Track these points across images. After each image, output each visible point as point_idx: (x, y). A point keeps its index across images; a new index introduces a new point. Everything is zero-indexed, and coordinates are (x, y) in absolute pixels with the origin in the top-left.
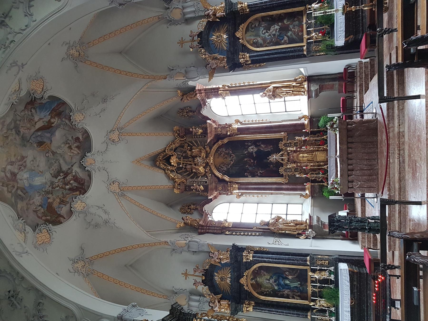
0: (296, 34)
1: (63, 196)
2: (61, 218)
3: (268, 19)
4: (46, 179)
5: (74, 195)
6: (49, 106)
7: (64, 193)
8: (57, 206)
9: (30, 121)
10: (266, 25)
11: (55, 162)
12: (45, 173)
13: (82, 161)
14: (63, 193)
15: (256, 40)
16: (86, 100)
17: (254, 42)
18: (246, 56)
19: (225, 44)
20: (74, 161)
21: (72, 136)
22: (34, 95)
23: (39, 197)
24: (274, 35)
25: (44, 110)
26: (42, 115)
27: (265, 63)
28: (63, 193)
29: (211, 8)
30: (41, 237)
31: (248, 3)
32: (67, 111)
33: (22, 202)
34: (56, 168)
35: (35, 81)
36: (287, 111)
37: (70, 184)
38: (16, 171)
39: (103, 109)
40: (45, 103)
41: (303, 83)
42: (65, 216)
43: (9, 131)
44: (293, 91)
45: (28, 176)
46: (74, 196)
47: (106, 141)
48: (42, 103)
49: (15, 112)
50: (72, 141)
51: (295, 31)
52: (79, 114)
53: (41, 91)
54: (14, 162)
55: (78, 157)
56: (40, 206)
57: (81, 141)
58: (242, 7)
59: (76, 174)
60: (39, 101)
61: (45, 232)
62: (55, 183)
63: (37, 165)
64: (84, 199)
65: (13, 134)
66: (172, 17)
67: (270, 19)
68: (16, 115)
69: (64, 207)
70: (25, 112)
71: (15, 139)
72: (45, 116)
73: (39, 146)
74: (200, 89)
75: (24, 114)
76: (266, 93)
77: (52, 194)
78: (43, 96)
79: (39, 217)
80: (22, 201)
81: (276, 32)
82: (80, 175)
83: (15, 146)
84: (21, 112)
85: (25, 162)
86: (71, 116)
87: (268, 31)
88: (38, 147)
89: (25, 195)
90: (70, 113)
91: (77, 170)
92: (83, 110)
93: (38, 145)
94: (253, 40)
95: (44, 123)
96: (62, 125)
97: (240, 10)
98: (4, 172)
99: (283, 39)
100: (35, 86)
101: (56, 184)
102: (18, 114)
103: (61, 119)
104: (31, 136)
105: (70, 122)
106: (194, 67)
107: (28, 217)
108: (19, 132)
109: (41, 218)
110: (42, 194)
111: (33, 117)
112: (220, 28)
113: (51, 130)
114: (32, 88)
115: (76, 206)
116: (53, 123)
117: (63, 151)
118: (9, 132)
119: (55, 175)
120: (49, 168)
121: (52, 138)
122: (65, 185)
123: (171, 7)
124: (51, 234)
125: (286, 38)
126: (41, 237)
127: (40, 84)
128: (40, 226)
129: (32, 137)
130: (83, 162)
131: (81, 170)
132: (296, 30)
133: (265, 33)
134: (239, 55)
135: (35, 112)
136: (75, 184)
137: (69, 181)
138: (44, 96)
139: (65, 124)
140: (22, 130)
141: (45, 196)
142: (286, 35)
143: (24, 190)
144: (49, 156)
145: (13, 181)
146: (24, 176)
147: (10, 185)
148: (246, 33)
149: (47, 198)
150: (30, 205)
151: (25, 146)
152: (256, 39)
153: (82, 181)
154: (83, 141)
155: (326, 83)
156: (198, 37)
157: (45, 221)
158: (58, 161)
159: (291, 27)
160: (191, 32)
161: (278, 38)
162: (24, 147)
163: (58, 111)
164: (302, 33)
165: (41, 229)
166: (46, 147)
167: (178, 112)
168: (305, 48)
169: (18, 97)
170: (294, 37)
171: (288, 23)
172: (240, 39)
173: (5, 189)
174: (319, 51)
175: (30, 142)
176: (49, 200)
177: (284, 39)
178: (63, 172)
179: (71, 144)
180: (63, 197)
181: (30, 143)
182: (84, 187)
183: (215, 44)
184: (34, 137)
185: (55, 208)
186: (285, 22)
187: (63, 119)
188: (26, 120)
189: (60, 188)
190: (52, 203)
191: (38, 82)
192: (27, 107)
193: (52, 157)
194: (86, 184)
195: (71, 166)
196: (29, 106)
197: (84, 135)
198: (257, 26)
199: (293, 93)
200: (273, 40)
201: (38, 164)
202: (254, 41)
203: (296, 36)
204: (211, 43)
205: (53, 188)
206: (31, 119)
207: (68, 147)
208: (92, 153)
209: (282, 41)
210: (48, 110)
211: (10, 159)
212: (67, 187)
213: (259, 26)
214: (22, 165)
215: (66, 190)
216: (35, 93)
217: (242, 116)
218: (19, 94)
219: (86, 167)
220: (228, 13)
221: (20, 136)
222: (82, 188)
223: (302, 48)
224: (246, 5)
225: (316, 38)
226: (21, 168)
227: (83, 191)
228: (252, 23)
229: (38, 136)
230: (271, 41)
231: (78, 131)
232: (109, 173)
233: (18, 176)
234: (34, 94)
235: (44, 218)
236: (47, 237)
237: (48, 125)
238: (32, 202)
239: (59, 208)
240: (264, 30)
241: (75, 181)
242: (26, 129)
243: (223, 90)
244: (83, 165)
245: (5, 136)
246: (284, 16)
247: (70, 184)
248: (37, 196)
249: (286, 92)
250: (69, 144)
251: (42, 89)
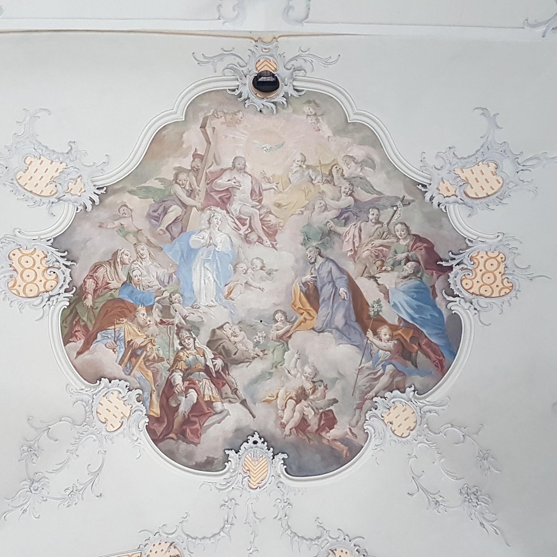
1: (151, 358)
2: (80, 343)
4: (206, 309)
5: (151, 396)
6: (429, 317)
7: (159, 364)
8: (122, 334)
9: (377, 256)
11: (257, 344)
12: (225, 307)
13: (258, 440)
14: (161, 359)
16: (461, 434)
20: (260, 410)
21: (337, 401)
22: (458, 264)
23: (157, 278)
25: (415, 303)
26: (400, 298)
28: (161, 359)
30: (34, 265)
32: (418, 380)
33: (146, 214)
34: (239, 346)
35: (501, 269)
37: (187, 389)
38: (235, 207)
39: (440, 499)
40: (435, 307)
42: (86, 356)
43: (347, 184)
45: (219, 248)
46: (146, 395)
47: (326, 536)
48: (435, 295)
49: (403, 200)
50: (321, 403)
52: (413, 419)
53: (471, 291)
54: (260, 201)
55: (271, 427)
56: (130, 278)
57: (323, 434)
59: (217, 413)
60: (439, 284)
61: (45, 284)
62: (195, 339)
63: (250, 281)
64: (134, 430)
65: (338, 200)
68: (393, 206)
69: (115, 356)
70: (405, 238)
71: (326, 208)
72: (395, 306)
73: (304, 289)
75: (398, 234)
77: (162, 322)
78: (458, 296)
79: (96, 267)
80: (149, 216)
82: (212, 428)
83: (305, 207)
84: (401, 223)
85: (260, 240)
86: (404, 392)
88: (301, 285)
89: (164, 229)
90: (413, 389)
91: (228, 416)
92: (428, 427)
93: (308, 289)
95: (376, 305)
96: (371, 362)
98: (234, 166)
100: (484, 270)
101: (192, 340)
102: (396, 211)
103: (391, 358)
104: (332, 261)
105: (384, 389)
107: (100, 227)
108: (347, 219)
109: (92, 277)
110: (163, 289)
111: (390, 269)
113: (354, 328)
114: (478, 257)
115: (113, 397)
116: (375, 333)
117: (292, 372)
118: (345, 186)
119: (221, 339)
120: (240, 323)
121: (331, 332)
122: (187, 370)
124: (37, 301)
126: (34, 265)
127: (494, 286)
128: (67, 266)
129: (331, 264)
130: (255, 442)
131: (230, 435)
135: (405, 274)
136: (184, 407)
137: (195, 384)
138: (457, 299)
139: (375, 374)
140: (351, 230)
141: (157, 298)
143: (180, 230)
144: (278, 322)
145: (207, 194)
146: (220, 233)
147: (195, 184)
149: (151, 303)
150: (135, 244)
151: (307, 239)
153: (191, 430)
154: (325, 442)
157: (81, 287)
158: (261, 354)
162: (302, 238)
163: (416, 348)
165: (59, 268)
166: (302, 314)
169: (447, 198)
173: (187, 163)
175: (315, 260)
176: (142, 310)
178: (225, 368)
179: (311, 397)
180: (146, 359)
181: (313, 260)
182: (171, 435)
184: (330, 272)
185: (117, 326)
187: (389, 368)
188: (380, 241)
189: (178, 352)
190: (133, 319)
191: (499, 276)
192: (419, 244)
193: (274, 334)
194: (183, 446)
195: (244, 398)
196: (423, 251)
197: (342, 446)
201: (254, 284)
205: (179, 328)
206: (383, 262)
207: (303, 389)
208: (283, 479)
210: (416, 316)
211: (270, 189)
212: (178, 377)
214: (252, 230)
215: (169, 370)
216: (462, 269)
218: (456, 202)
219: (236, 453)
221: (332, 223)
222: (169, 429)
226: (244, 225)
227: (159, 429)
229: (334, 286)
231: (354, 422)
232: (212, 540)
233: (220, 213)
234: (461, 266)
235: (90, 285)
236: (29, 287)
237: (369, 317)
238: (142, 252)
239: (116, 340)
241: (196, 403)
242: (354, 243)
244: (245, 444)
245: (334, 171)
247: (187, 389)
248: (161, 272)
250: (313, 392)
251: (478, 293)
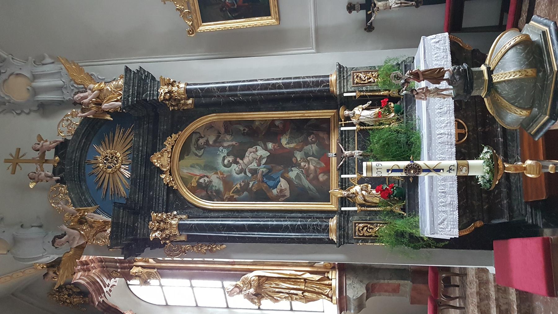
0: (312, 176)
3: (242, 128)
10: (234, 143)
15: (207, 179)
17: (199, 185)
18: (171, 224)
19: (124, 180)
24: (254, 172)
27: (224, 246)
29: (92, 86)
31: (188, 84)
36: (293, 309)
41: (328, 272)
44: (304, 291)
51: (309, 167)
58: (170, 92)
66: (6, 96)
67: (247, 129)
74: (86, 261)
76: (242, 285)
81: (259, 165)
87: (238, 160)
94: (198, 177)
97: (165, 99)
99: (275, 187)
106: (40, 227)
112: (116, 138)
123: (4, 72)
125: (283, 184)
132: (312, 167)
133: (229, 165)
134: (150, 219)
142: (286, 175)
148: (181, 158)
152: (207, 177)
155: (382, 281)
156: (56, 154)
159: (298, 156)
160: (40, 138)
161: (263, 181)
164: (326, 177)
167: (51, 294)
168: (333, 223)
170: (306, 183)
171: (292, 146)
172: (162, 172)
174: (374, 239)
177: (278, 187)
183: (100, 176)
186: (284, 141)
198: (211, 143)
199: (304, 296)
200: (250, 186)
202: (202, 181)
203: (310, 182)
204: (88, 172)
209: (275, 191)
213: (217, 144)
217: (196, 308)
220: (130, 103)
223: (325, 224)
224: (182, 90)
225: (365, 200)
228: (198, 135)
230: (245, 188)
240: (228, 155)
243: (143, 267)
246: (281, 126)
249: (287, 291)
